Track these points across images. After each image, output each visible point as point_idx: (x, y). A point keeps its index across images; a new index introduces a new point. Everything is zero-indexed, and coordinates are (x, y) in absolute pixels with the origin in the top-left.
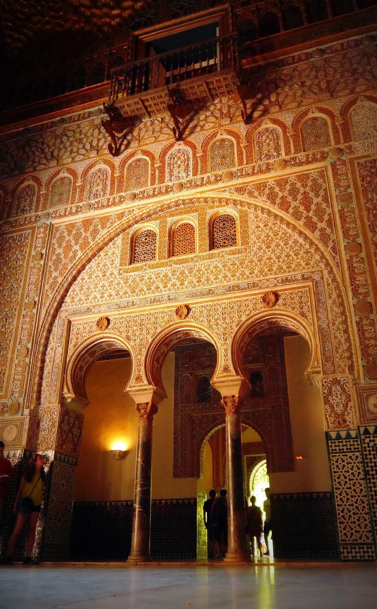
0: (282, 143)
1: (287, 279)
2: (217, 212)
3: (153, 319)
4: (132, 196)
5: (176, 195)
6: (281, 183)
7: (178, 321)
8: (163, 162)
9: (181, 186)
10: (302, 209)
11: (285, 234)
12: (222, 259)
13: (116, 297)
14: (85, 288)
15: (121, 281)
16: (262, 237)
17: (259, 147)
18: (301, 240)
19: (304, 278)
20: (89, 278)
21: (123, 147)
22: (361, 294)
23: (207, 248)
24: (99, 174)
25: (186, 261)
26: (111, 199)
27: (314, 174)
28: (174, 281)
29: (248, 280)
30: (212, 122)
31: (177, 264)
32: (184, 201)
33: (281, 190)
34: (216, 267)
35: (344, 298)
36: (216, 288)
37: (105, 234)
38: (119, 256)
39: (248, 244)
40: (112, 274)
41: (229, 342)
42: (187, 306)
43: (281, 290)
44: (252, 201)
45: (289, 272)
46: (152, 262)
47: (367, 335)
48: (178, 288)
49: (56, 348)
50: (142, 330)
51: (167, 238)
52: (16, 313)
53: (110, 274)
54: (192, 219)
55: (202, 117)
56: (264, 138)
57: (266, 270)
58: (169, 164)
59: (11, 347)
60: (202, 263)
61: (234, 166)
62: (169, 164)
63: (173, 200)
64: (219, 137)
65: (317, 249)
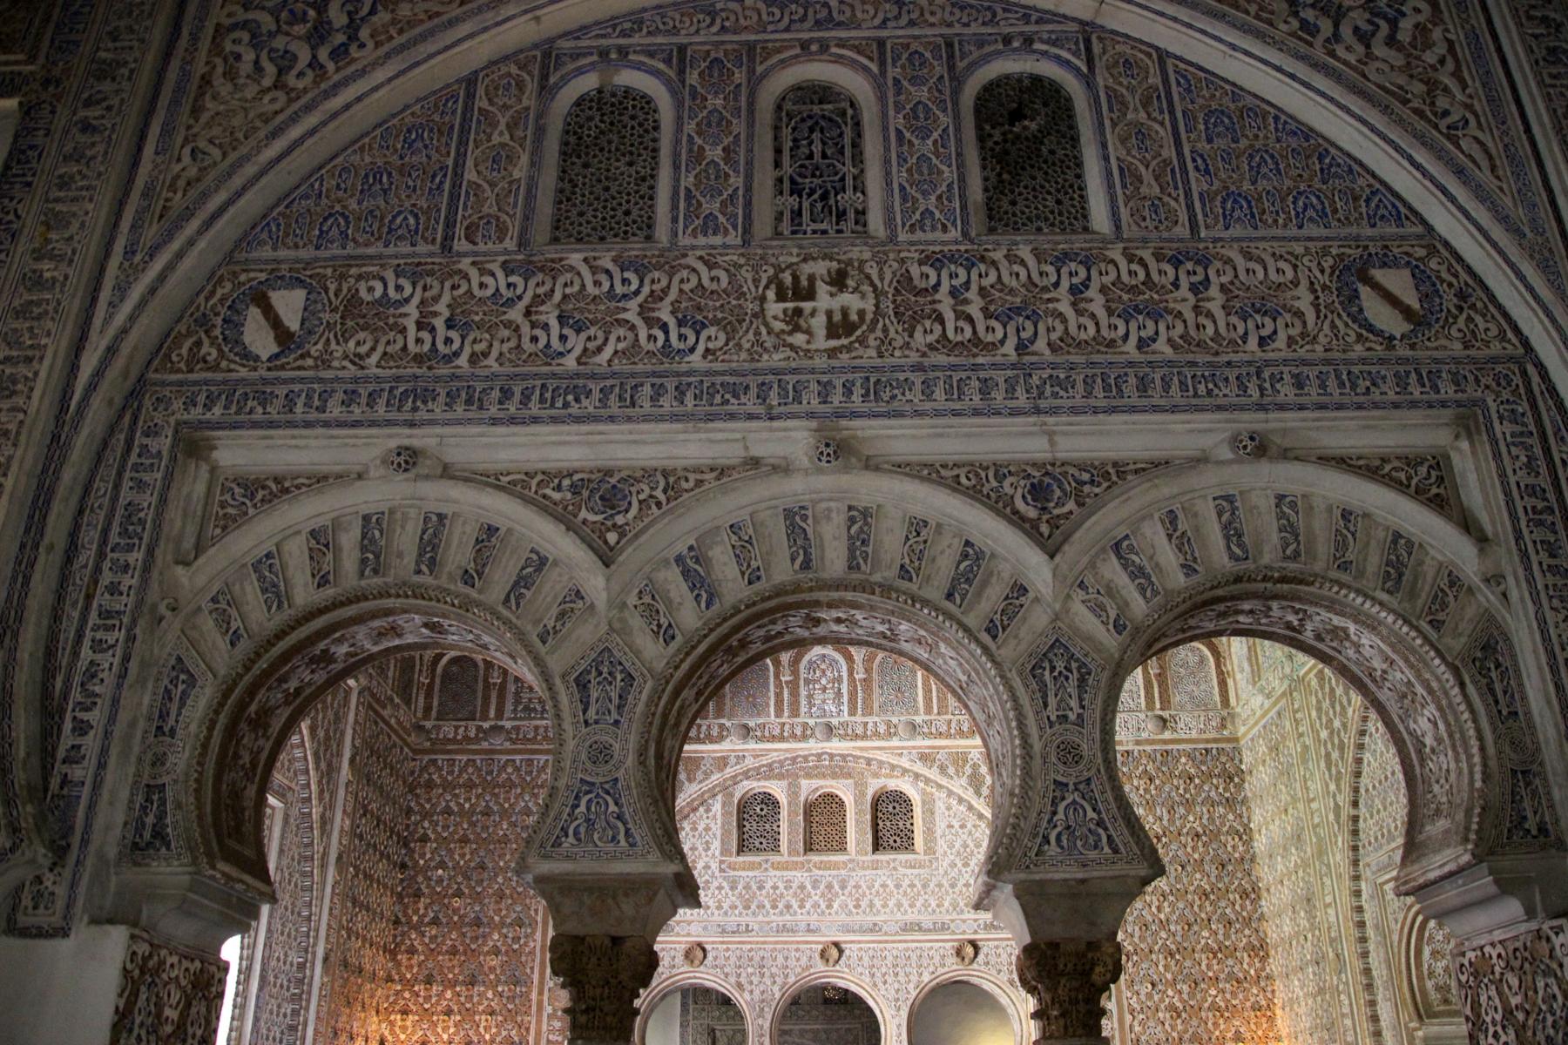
3: (780, 959)
5: (820, 745)
8: (795, 673)
9: (830, 730)
15: (725, 884)
16: (957, 845)
23: (870, 848)
25: (836, 866)
32: (832, 756)
34: (884, 886)
41: (904, 1014)
42: (836, 944)
44: (944, 781)
46: (777, 858)
50: (762, 975)
51: (801, 817)
52: (539, 919)
54: (844, 790)
58: (807, 682)
59: (536, 981)
61: (916, 713)
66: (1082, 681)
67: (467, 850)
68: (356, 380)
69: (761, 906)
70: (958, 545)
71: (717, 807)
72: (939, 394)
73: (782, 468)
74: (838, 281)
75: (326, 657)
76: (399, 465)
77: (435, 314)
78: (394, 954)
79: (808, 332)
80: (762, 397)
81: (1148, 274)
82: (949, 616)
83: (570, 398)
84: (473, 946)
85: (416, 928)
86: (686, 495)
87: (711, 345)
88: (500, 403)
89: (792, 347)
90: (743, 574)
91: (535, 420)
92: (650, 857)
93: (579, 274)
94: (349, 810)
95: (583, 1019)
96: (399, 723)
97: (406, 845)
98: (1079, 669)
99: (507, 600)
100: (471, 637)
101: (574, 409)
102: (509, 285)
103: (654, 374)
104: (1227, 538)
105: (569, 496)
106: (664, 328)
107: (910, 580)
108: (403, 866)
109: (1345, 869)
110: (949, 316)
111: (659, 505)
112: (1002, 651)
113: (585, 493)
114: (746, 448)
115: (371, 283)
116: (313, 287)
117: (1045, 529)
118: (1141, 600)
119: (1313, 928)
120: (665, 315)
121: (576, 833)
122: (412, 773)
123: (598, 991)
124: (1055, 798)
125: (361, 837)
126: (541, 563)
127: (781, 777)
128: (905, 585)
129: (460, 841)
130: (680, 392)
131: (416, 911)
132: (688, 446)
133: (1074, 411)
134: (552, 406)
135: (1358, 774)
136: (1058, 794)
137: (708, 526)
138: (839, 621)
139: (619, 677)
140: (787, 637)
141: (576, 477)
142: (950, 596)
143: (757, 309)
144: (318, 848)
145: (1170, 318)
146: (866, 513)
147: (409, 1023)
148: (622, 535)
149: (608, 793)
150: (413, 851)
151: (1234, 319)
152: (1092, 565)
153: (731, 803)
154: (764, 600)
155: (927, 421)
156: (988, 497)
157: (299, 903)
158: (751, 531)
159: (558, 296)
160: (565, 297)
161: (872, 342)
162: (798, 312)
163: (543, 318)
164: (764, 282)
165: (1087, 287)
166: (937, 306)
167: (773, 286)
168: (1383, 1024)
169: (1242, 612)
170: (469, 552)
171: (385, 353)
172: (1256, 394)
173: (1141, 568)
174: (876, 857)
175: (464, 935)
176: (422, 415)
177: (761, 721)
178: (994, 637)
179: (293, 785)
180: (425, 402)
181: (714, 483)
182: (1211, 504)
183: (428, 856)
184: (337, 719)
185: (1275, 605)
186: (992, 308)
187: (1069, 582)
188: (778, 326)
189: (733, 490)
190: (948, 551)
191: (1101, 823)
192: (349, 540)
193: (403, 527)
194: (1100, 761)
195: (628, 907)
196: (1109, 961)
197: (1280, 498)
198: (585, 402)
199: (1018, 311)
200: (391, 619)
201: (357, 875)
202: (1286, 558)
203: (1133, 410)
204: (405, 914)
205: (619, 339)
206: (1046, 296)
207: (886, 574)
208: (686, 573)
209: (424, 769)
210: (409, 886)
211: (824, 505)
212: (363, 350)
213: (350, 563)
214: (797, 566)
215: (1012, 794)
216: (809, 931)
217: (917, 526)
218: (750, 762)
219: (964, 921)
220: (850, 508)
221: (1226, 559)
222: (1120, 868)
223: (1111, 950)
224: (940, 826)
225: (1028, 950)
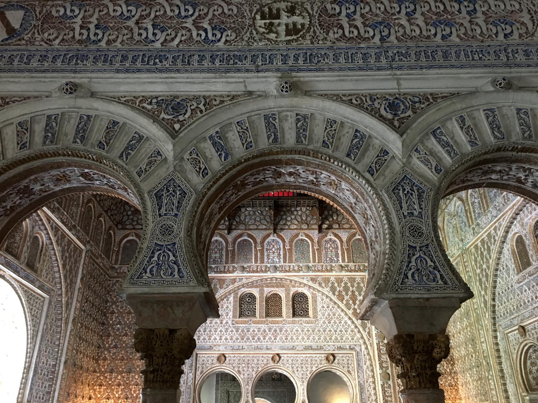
0: (340, 252)
1: (340, 347)
3: (256, 361)
4: (242, 269)
6: (339, 280)
7: (273, 365)
8: (263, 246)
9: (276, 269)
10: (351, 302)
11: (340, 315)
13: (230, 341)
14: (207, 330)
15: (234, 330)
18: (349, 322)
19: (351, 349)
20: (210, 323)
21: (233, 227)
22: (384, 367)
23: (291, 315)
25: (278, 322)
26: (227, 267)
27: (358, 279)
28: (270, 335)
29: (317, 344)
30: (295, 224)
31: (271, 323)
32: (276, 279)
33: (338, 286)
34: (297, 331)
35: (374, 366)
36: (298, 345)
38: (232, 310)
40: (227, 323)
41: (305, 384)
42: (278, 355)
43: (336, 354)
44: (320, 289)
45: (342, 342)
46: (254, 319)
47: (387, 394)
48: (273, 341)
49: (188, 374)
50: (248, 367)
51: (264, 303)
55: (289, 219)
56: (329, 245)
57: (328, 339)
58: (267, 250)
61: (310, 262)
64: (300, 237)
65: (359, 332)
66: (420, 196)
67: (130, 317)
68: (47, 51)
69: (248, 339)
70: (352, 132)
71: (231, 299)
72: (342, 60)
73: (264, 96)
74: (291, 11)
75: (27, 191)
76: (67, 90)
77: (90, 22)
78: (97, 360)
79: (277, 33)
80: (254, 61)
81: (445, 7)
82: (348, 165)
83: (157, 60)
84: (131, 357)
85: (108, 349)
86: (215, 108)
87: (228, 39)
88: (121, 62)
89: (268, 39)
90: (243, 144)
91: (139, 71)
92: (191, 284)
93: (163, 6)
94: (79, 300)
95: (151, 376)
96: (104, 265)
97: (105, 315)
98: (418, 190)
99: (121, 156)
100: (105, 181)
101: (159, 65)
102: (128, 11)
103: (200, 51)
104: (492, 129)
105: (156, 107)
106: (206, 30)
107: (328, 147)
108: (103, 324)
109: (490, 327)
110: (346, 26)
111: (201, 111)
112: (376, 182)
113: (164, 106)
114: (246, 86)
115: (58, 8)
116: (28, 9)
117: (396, 123)
118: (448, 158)
119: (475, 352)
120: (206, 25)
121: (151, 271)
122: (109, 286)
123: (160, 360)
124: (409, 254)
125: (84, 311)
126: (140, 138)
127: (256, 287)
128: (325, 150)
129: (128, 313)
130: (213, 59)
131: (108, 343)
132: (218, 85)
133: (410, 68)
134: (148, 64)
135: (495, 287)
136: (411, 252)
137: (227, 122)
138: (290, 174)
139: (178, 193)
140: (265, 184)
141: (159, 99)
142: (348, 155)
143: (251, 23)
144: (64, 315)
145: (457, 26)
146: (305, 117)
147: (102, 390)
148: (182, 126)
149: (170, 250)
150: (108, 318)
151: (490, 26)
152: (422, 142)
153: (237, 297)
154: (254, 157)
155: (336, 73)
156: (367, 109)
157: (54, 339)
158: (247, 125)
159: (152, 16)
160: (156, 16)
161: (308, 37)
162: (271, 24)
163: (145, 25)
164: (255, 11)
165: (415, 14)
166: (340, 22)
167: (259, 13)
168: (509, 393)
169: (493, 172)
170: (103, 133)
171: (63, 39)
172: (505, 59)
173: (447, 143)
175: (127, 352)
176: (80, 66)
177: (249, 265)
178: (372, 175)
179: (54, 289)
180: (82, 61)
181: (229, 102)
182: (482, 113)
183: (114, 319)
184: (76, 262)
185: (514, 166)
186: (367, 23)
187: (410, 148)
188: (262, 30)
189: (239, 104)
190: (347, 135)
191: (435, 268)
192: (39, 128)
193: (69, 122)
194: (433, 235)
195: (179, 312)
196: (443, 345)
197: (519, 110)
198: (165, 63)
199: (381, 23)
200: (62, 170)
201: (82, 327)
202: (525, 138)
203: (441, 67)
204: (103, 344)
205: (182, 35)
206: (395, 17)
207: (315, 145)
208: (214, 144)
209: (114, 284)
210: (105, 332)
211: (284, 114)
212: (51, 37)
213: (38, 138)
214: (271, 141)
215: (384, 254)
216: (267, 349)
217: (331, 123)
218: (244, 281)
219: (329, 346)
220: (297, 115)
221: (492, 139)
222: (449, 293)
223: (443, 339)
224: (319, 307)
225: (397, 338)
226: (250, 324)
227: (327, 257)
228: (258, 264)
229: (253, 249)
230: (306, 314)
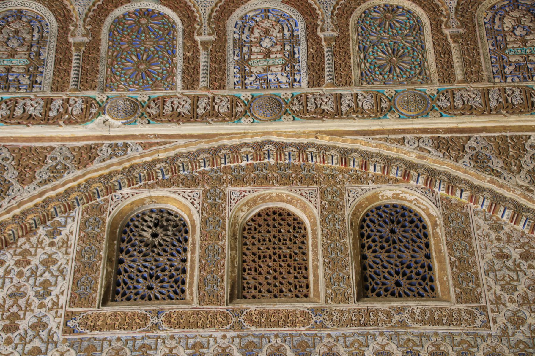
2: (375, 197)
5: (260, 127)
8: (221, 33)
9: (278, 109)
12: (400, 331)
17: (496, 44)
24: (16, 25)
25: (288, 319)
31: (259, 324)
32: (280, 147)
37: (31, 200)
39: (477, 299)
40: (39, 325)
44: (484, 181)
53: (33, 327)
56: (508, 23)
58: (239, 44)
60: (339, 333)
61: (427, 80)
62: (239, 44)
63: (249, 140)
71: (72, 228)
127: (191, 182)
174: (366, 305)
218: (137, 156)
224: (483, 256)
226: (156, 326)
227: (503, 63)
228: (198, 92)
229: (180, 40)
230: (421, 283)
